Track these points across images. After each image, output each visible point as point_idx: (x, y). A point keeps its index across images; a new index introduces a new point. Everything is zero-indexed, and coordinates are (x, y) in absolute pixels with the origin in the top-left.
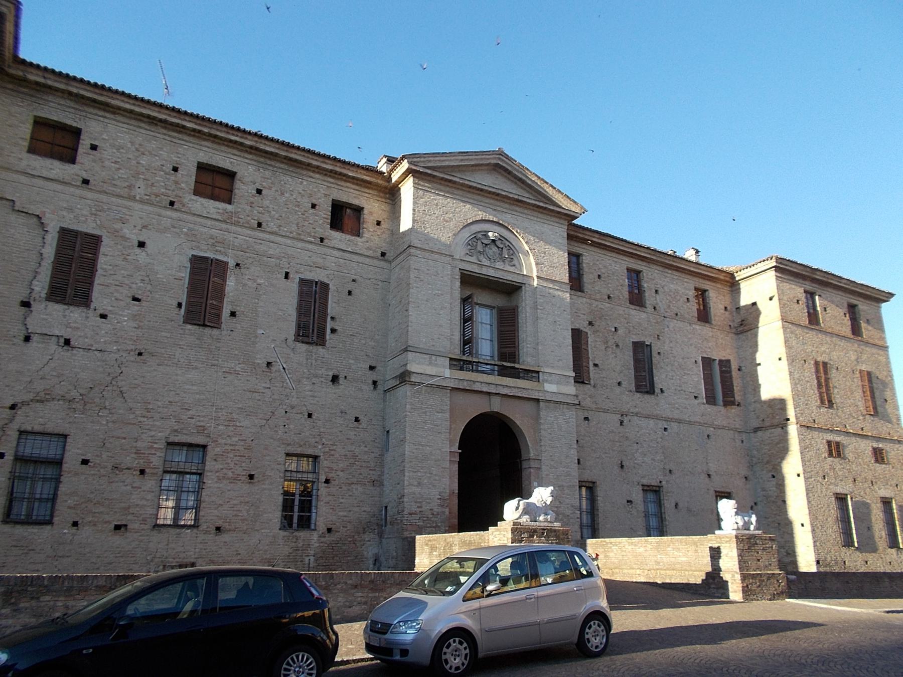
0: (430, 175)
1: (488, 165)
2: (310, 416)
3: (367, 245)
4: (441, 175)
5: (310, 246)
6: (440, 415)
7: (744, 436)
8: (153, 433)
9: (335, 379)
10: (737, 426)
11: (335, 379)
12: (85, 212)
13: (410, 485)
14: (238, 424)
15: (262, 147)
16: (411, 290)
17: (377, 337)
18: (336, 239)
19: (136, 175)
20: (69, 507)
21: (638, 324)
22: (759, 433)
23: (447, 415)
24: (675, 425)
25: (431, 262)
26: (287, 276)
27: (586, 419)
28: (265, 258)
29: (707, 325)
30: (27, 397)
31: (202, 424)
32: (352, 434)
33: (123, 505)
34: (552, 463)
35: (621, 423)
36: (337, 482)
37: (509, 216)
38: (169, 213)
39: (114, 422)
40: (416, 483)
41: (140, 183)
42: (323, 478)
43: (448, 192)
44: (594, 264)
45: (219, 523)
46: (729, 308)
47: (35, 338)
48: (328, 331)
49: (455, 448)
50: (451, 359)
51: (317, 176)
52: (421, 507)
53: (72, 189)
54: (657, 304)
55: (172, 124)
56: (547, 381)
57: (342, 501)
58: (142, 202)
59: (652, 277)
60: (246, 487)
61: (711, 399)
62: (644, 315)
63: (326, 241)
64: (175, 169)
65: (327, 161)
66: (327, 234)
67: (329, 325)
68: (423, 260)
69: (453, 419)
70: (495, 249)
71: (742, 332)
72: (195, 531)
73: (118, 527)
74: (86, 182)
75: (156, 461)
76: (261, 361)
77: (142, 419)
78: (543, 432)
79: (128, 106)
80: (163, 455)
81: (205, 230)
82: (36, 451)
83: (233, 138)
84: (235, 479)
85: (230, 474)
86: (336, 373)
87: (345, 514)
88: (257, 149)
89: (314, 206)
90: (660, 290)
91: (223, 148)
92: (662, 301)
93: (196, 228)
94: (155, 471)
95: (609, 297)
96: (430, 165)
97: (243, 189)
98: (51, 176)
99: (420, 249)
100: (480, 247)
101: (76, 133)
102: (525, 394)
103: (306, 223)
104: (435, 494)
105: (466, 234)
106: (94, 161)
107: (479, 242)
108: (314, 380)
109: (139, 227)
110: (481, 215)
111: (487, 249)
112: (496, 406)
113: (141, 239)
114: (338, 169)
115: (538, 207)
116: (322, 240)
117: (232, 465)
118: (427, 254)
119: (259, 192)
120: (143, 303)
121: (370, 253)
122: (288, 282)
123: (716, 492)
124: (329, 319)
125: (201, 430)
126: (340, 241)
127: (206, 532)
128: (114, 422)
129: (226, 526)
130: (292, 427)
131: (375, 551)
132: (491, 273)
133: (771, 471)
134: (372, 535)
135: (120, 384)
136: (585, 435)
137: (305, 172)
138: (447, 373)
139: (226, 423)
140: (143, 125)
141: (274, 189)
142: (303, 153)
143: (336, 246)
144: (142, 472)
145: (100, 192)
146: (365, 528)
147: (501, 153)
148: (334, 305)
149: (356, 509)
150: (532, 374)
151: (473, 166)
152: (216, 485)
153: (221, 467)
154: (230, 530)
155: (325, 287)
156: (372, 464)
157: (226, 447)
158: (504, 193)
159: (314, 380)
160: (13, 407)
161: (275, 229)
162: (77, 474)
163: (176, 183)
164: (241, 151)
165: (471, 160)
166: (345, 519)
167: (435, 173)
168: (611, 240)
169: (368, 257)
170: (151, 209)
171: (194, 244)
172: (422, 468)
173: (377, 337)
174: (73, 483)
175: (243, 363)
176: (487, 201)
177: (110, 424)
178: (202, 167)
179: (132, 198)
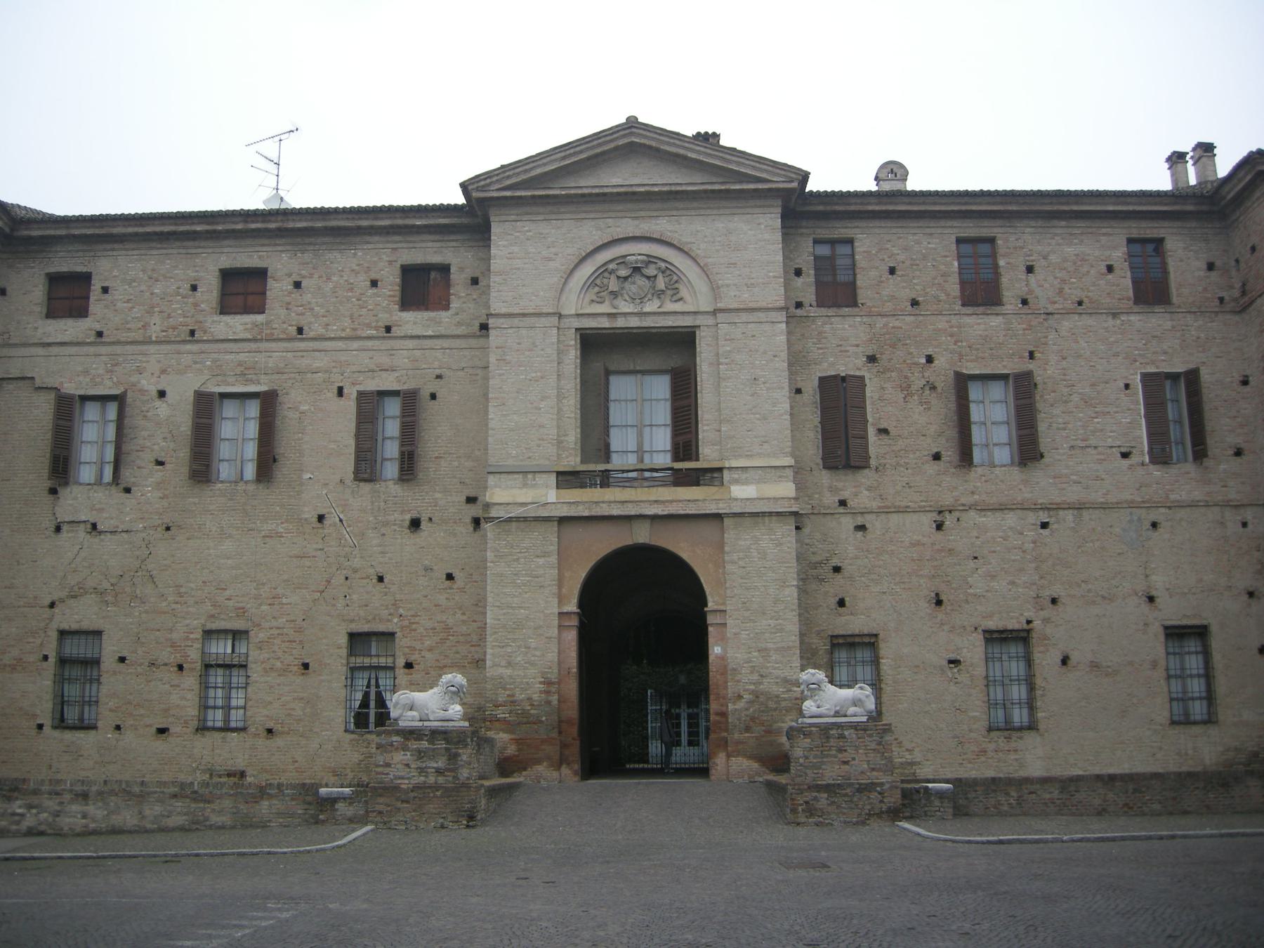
0: (512, 198)
1: (616, 148)
2: (381, 579)
3: (457, 319)
4: (529, 193)
5: (370, 343)
6: (541, 561)
7: (1249, 514)
8: (188, 622)
9: (415, 524)
11: (415, 524)
12: (101, 371)
13: (495, 665)
14: (284, 600)
15: (291, 225)
16: (491, 382)
17: (477, 453)
18: (408, 322)
19: (150, 312)
20: (111, 710)
21: (987, 339)
23: (554, 559)
24: (1069, 516)
25: (524, 332)
26: (340, 392)
27: (861, 528)
28: (309, 375)
30: (63, 594)
31: (241, 605)
32: (442, 599)
33: (162, 706)
34: (747, 614)
35: (939, 527)
36: (422, 666)
38: (188, 347)
39: (146, 612)
40: (503, 663)
41: (156, 319)
42: (401, 662)
44: (880, 250)
45: (270, 725)
46: (1218, 263)
47: (65, 528)
49: (572, 607)
50: (559, 473)
51: (376, 238)
52: (513, 696)
53: (85, 349)
54: (1031, 292)
55: (182, 233)
56: (737, 482)
58: (158, 342)
59: (1020, 243)
60: (299, 680)
61: (1160, 457)
62: (995, 321)
63: (393, 329)
64: (194, 288)
66: (395, 318)
68: (510, 331)
70: (641, 281)
72: (242, 734)
73: (162, 731)
74: (100, 334)
75: (194, 654)
76: (310, 514)
77: (174, 606)
78: (729, 567)
79: (130, 230)
80: (200, 646)
81: (232, 357)
82: (75, 651)
83: (253, 226)
84: (284, 671)
85: (278, 664)
86: (415, 515)
88: (287, 230)
89: (374, 283)
90: (1039, 265)
91: (249, 242)
92: (1042, 287)
93: (221, 356)
94: (193, 666)
95: (915, 303)
96: (509, 182)
97: (277, 289)
98: (66, 339)
100: (613, 285)
101: (86, 278)
102: (692, 510)
103: (364, 311)
105: (587, 269)
106: (106, 307)
107: (613, 277)
108: (383, 530)
109: (157, 373)
110: (599, 238)
111: (627, 285)
112: (642, 535)
113: (160, 388)
115: (713, 191)
116: (388, 329)
117: (280, 654)
118: (516, 321)
119: (297, 285)
120: (168, 466)
121: (459, 331)
122: (342, 401)
125: (241, 612)
127: (256, 735)
128: (146, 612)
129: (278, 728)
130: (355, 597)
132: (634, 322)
135: (150, 567)
137: (358, 239)
138: (552, 495)
139: (270, 601)
140: (154, 244)
141: (316, 276)
142: (345, 216)
143: (409, 333)
144: (181, 667)
145: (113, 343)
147: (632, 123)
150: (712, 475)
151: (588, 159)
152: (262, 679)
153: (267, 656)
154: (283, 733)
157: (272, 632)
158: (642, 189)
159: (383, 530)
160: (52, 605)
161: (321, 331)
162: (115, 673)
163: (196, 305)
164: (270, 237)
165: (581, 152)
167: (518, 193)
168: (906, 200)
169: (458, 337)
170: (169, 347)
171: (220, 378)
172: (514, 640)
173: (477, 453)
174: (113, 686)
175: (287, 521)
176: (620, 207)
177: (144, 615)
178: (228, 276)
179: (148, 341)
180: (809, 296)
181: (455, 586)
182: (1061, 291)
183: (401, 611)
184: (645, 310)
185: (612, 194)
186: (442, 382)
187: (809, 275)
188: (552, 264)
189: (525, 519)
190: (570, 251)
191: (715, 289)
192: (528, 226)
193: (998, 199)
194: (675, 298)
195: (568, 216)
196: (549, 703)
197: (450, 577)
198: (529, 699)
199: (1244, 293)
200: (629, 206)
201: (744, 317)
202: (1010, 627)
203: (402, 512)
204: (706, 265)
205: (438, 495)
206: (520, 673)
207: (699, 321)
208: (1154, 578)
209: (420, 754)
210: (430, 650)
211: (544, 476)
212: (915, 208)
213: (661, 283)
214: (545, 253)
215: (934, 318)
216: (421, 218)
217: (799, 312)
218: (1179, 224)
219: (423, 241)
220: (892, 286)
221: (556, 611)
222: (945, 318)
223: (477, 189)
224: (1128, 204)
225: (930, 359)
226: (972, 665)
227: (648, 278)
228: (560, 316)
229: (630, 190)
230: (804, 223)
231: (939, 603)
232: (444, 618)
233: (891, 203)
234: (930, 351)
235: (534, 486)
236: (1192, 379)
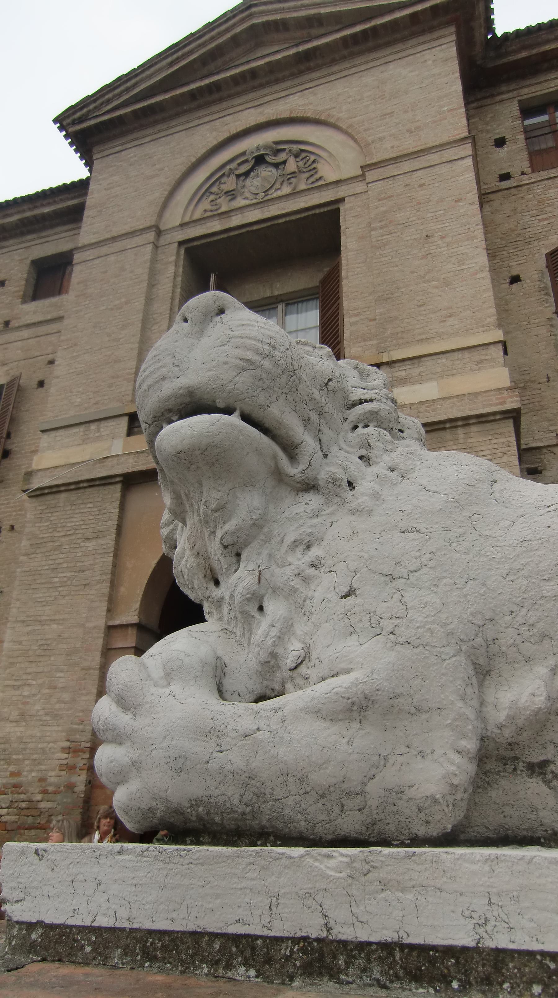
1: (234, 38)
6: (90, 545)
40: (15, 714)
51: (11, 242)
52: (17, 774)
65: (9, 212)
68: (97, 261)
100: (230, 183)
111: (248, 182)
114: (28, 214)
116: (7, 323)
118: (104, 250)
126: (35, 312)
180: (514, 157)
187: (515, 141)
191: (363, 147)
196: (70, 787)
198: (42, 780)
204: (351, 126)
213: (292, 165)
216: (49, 204)
217: (506, 184)
219: (56, 234)
221: (101, 623)
223: (74, 123)
227: (276, 166)
228: (159, 233)
230: (504, 88)
235: (97, 439)
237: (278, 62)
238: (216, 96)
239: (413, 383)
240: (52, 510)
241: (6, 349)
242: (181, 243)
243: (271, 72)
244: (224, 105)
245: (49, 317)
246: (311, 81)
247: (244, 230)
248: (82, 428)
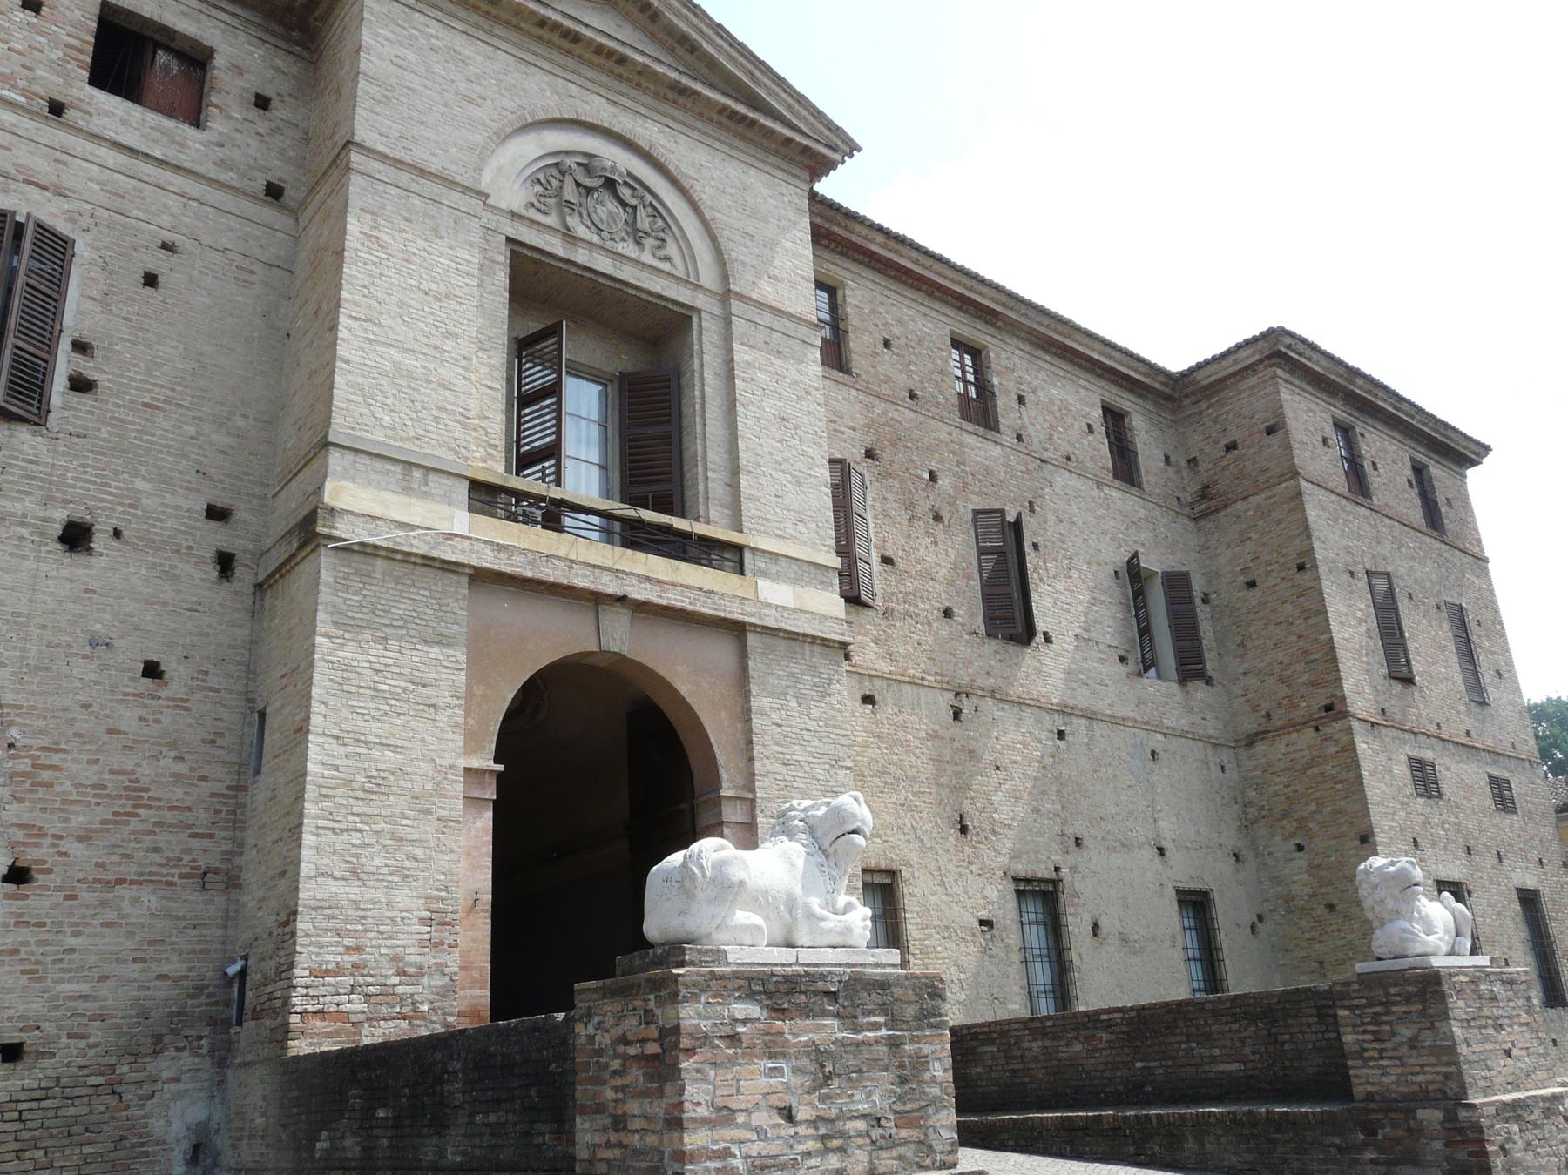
3: (221, 153)
9: (76, 537)
10: (1211, 732)
17: (240, 422)
22: (1260, 747)
25: (417, 201)
27: (868, 699)
29: (1134, 490)
32: (128, 718)
36: (56, 879)
37: (656, 127)
43: (478, 27)
44: (873, 311)
46: (1173, 459)
48: (60, 382)
49: (485, 760)
50: (476, 486)
52: (359, 949)
54: (1024, 427)
56: (764, 574)
57: (72, 942)
62: (996, 451)
63: (70, 114)
66: (75, 92)
67: (64, 363)
68: (393, 191)
69: (478, 667)
71: (1204, 515)
86: (79, 513)
87: (84, 988)
90: (1029, 398)
92: (1034, 422)
95: (912, 396)
99: (384, 158)
100: (570, 193)
104: (410, 901)
105: (531, 148)
107: (568, 181)
111: (591, 203)
118: (404, 178)
121: (225, 176)
123: (1178, 891)
124: (65, 345)
126: (123, 122)
131: (197, 1113)
132: (604, 264)
133: (1293, 835)
134: (187, 1060)
136: (866, 745)
146: (157, 1035)
148: (88, 305)
149: (132, 970)
155: (55, 248)
156: (202, 817)
166: (81, 1006)
168: (915, 255)
173: (240, 422)
176: (592, 74)
181: (164, 693)
182: (1051, 438)
183: (14, 732)
184: (619, 250)
185: (590, 41)
186: (174, 259)
188: (476, 112)
189: (407, 558)
190: (506, 103)
192: (434, 28)
193: (1003, 298)
194: (661, 253)
195: (504, 46)
197: (152, 670)
198: (396, 958)
199: (1203, 497)
200: (605, 79)
201: (767, 319)
202: (1040, 875)
203: (46, 501)
205: (140, 485)
206: (379, 895)
207: (700, 301)
208: (1161, 823)
209: (825, 1069)
210: (81, 839)
211: (444, 480)
212: (920, 271)
214: (463, 86)
215: (933, 422)
218: (1138, 401)
220: (887, 363)
222: (947, 428)
224: (1111, 358)
225: (933, 477)
226: (1005, 929)
227: (624, 205)
229: (622, 49)
231: (964, 830)
232: (129, 765)
233: (895, 252)
234: (933, 465)
235: (426, 495)
236: (1177, 584)
237: (656, 73)
238: (566, 44)
239: (773, 580)
240: (364, 579)
241: (65, 164)
242: (509, 239)
243: (639, 73)
244: (570, 62)
245: (158, 154)
246: (674, 119)
247: (587, 274)
248: (398, 468)
